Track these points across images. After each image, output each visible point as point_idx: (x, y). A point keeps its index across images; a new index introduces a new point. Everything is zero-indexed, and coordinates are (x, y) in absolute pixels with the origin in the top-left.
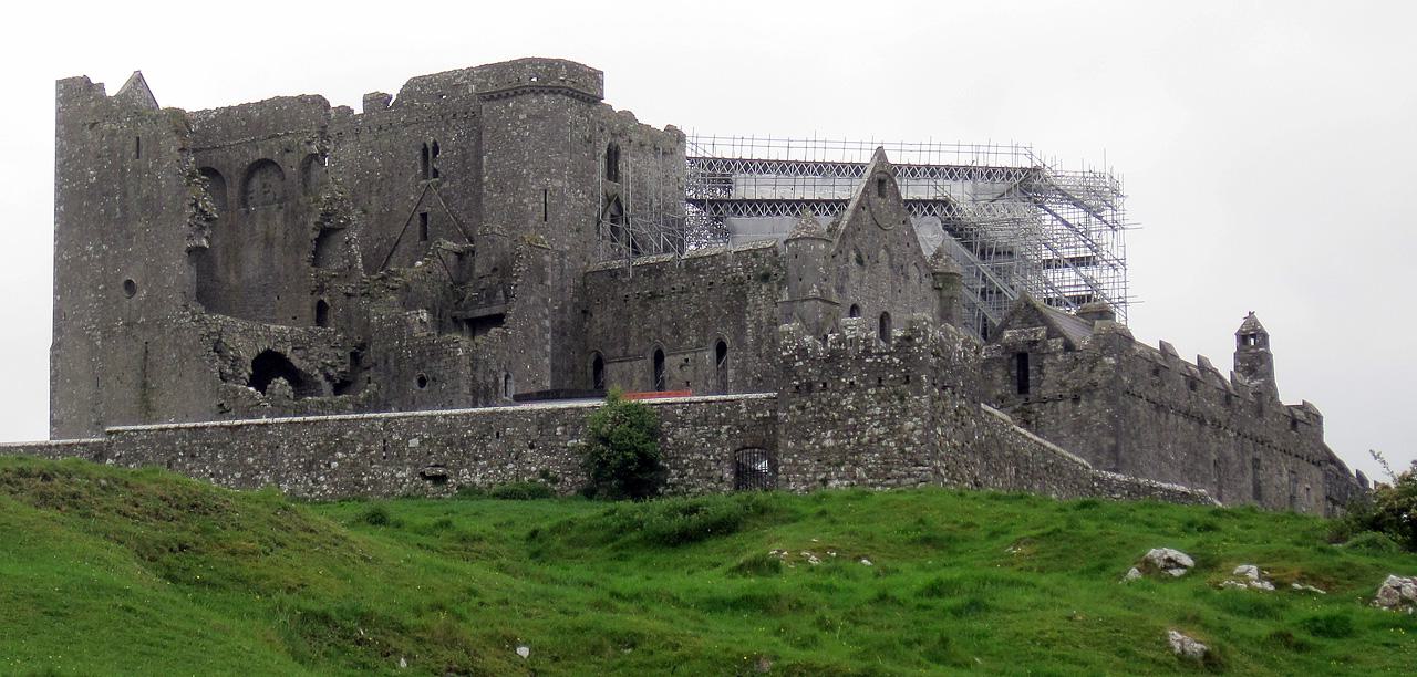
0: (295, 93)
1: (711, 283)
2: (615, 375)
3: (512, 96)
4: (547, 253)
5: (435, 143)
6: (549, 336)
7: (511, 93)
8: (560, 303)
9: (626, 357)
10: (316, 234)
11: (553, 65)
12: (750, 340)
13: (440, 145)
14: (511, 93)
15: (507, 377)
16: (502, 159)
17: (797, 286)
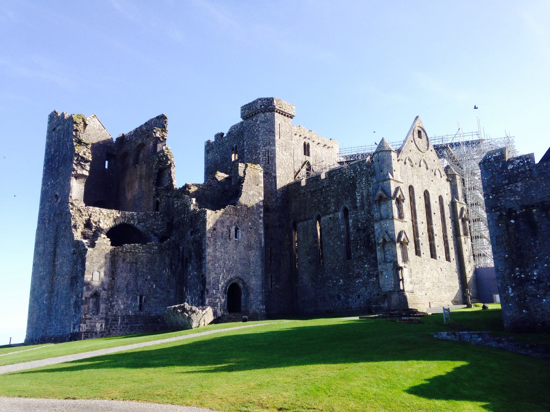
1: (339, 181)
5: (236, 146)
6: (262, 210)
8: (275, 198)
10: (157, 171)
12: (358, 205)
13: (237, 146)
15: (236, 230)
16: (251, 142)
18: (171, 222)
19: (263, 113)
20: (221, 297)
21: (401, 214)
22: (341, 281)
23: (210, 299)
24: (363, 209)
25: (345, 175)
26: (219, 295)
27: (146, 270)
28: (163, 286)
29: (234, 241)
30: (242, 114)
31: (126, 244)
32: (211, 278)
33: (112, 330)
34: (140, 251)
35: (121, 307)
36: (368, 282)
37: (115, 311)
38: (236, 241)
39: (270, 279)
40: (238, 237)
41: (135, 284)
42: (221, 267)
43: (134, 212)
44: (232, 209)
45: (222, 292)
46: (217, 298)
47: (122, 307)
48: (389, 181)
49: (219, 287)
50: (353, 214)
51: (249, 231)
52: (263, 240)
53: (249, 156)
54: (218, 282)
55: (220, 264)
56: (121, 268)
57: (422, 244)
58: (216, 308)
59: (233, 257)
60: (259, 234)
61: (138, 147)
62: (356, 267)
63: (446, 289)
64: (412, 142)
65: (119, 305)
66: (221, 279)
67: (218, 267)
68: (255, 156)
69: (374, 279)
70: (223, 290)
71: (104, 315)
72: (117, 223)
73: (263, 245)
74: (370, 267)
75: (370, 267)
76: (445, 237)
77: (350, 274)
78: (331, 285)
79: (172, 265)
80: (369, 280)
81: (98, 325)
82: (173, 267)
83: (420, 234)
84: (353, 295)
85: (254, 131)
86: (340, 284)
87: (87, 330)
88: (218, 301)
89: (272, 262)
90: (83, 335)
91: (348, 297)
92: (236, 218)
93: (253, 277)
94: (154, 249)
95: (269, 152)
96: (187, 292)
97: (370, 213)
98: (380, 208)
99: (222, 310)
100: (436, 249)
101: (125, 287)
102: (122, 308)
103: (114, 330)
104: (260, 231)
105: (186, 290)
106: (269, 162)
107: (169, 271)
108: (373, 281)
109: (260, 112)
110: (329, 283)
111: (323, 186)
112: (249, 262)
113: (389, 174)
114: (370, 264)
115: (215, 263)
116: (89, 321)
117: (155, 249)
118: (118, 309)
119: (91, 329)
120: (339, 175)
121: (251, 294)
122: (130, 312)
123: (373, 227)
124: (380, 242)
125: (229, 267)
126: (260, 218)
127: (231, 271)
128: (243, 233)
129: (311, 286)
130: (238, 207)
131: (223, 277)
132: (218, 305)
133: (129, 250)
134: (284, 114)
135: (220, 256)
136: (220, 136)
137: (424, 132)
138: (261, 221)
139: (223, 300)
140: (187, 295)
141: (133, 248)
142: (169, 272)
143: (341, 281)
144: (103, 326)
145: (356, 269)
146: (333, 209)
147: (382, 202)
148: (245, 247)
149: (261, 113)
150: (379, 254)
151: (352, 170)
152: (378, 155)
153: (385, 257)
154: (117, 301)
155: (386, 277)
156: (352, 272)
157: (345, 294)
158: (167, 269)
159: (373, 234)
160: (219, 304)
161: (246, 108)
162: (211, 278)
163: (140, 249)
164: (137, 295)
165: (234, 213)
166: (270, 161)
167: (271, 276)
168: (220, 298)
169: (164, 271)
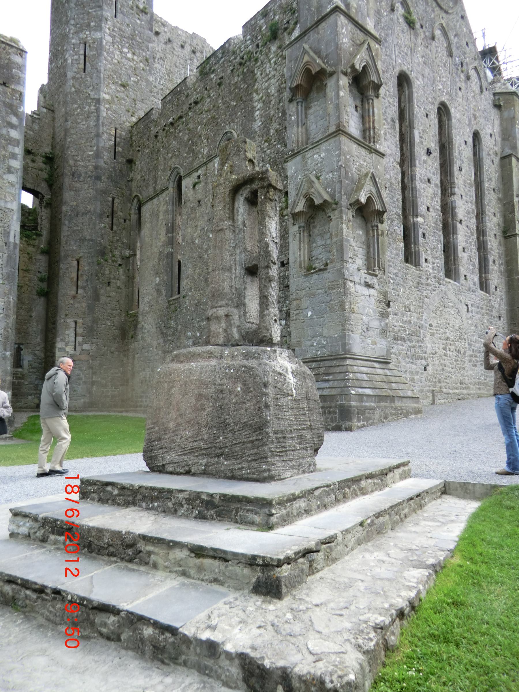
1: (221, 78)
57: (424, 235)
63: (476, 356)
76: (481, 232)
83: (422, 209)
100: (460, 256)
124: (297, 210)
146: (205, 152)
147: (314, 95)
151: (248, 37)
155: (310, 314)
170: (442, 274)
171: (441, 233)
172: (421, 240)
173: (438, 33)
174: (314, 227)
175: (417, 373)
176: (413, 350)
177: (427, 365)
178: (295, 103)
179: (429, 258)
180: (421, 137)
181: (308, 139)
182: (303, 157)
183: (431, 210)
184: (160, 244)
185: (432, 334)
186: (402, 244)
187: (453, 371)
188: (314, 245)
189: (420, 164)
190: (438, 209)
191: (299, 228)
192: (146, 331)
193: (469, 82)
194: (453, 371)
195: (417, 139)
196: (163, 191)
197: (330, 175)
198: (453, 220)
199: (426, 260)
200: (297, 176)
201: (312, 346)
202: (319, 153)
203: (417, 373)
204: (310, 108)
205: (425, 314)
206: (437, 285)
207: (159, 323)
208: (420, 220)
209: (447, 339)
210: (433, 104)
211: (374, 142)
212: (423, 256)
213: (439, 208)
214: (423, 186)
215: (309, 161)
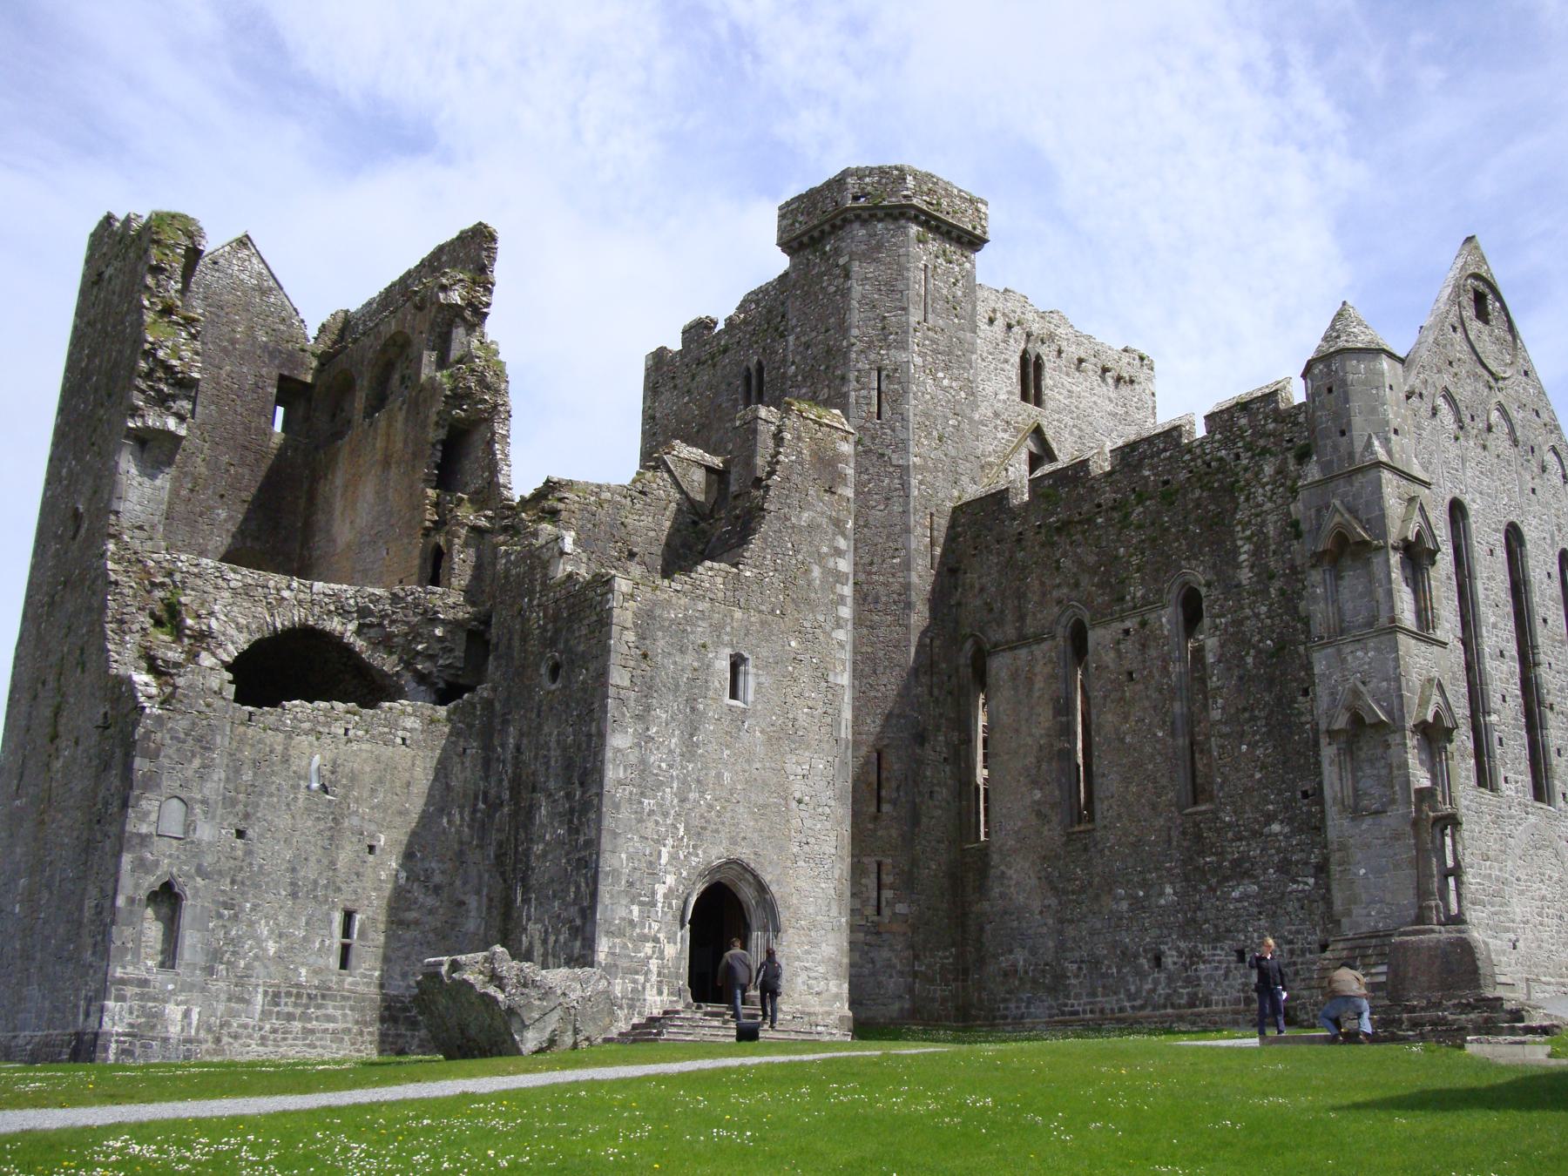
0: (453, 234)
1: (1166, 483)
2: (1004, 674)
3: (830, 233)
4: (846, 439)
5: (759, 363)
6: (847, 590)
7: (827, 227)
9: (1023, 640)
10: (442, 434)
11: (893, 176)
13: (764, 363)
14: (827, 227)
15: (737, 663)
16: (814, 334)
17: (1335, 448)
18: (482, 627)
19: (864, 222)
20: (661, 936)
21: (1426, 609)
22: (1169, 890)
23: (617, 940)
24: (1266, 591)
25: (1187, 457)
26: (655, 926)
27: (372, 808)
28: (437, 878)
29: (726, 709)
30: (782, 230)
31: (297, 702)
32: (624, 856)
33: (229, 1035)
34: (351, 733)
35: (265, 950)
36: (1283, 894)
37: (242, 964)
38: (731, 708)
39: (873, 877)
40: (741, 693)
41: (325, 862)
42: (665, 815)
43: (345, 587)
44: (719, 580)
45: (669, 917)
46: (644, 938)
47: (272, 947)
48: (1372, 474)
49: (653, 893)
50: (1224, 616)
51: (791, 674)
52: (847, 714)
53: (804, 391)
54: (654, 875)
55: (663, 799)
56: (271, 795)
57: (1500, 739)
58: (641, 978)
59: (719, 776)
60: (833, 689)
61: (384, 349)
62: (1230, 835)
64: (1454, 329)
65: (259, 941)
66: (664, 861)
67: (651, 812)
68: (826, 390)
69: (1306, 884)
70: (670, 906)
71: (198, 972)
72: (279, 625)
73: (846, 733)
74: (1293, 833)
75: (1293, 833)
77: (1206, 863)
78: (1124, 906)
79: (476, 798)
80: (1286, 886)
81: (174, 1011)
82: (481, 806)
83: (1495, 701)
84: (1215, 948)
85: (826, 294)
86: (1162, 902)
87: (131, 1025)
88: (650, 952)
89: (886, 808)
90: (113, 1045)
91: (1194, 956)
92: (738, 614)
93: (801, 863)
94: (405, 729)
95: (884, 373)
96: (529, 909)
97: (1296, 608)
98: (1337, 586)
99: (666, 991)
100: (1554, 763)
101: (287, 870)
102: (271, 952)
103: (236, 1037)
104: (836, 674)
105: (526, 901)
106: (883, 409)
107: (462, 818)
108: (1303, 891)
109: (851, 222)
110: (1118, 900)
111: (1099, 506)
112: (785, 799)
113: (1376, 443)
114: (1290, 821)
115: (643, 794)
116: (137, 990)
117: (411, 730)
118: (256, 957)
119: (147, 1023)
120: (1165, 459)
121: (791, 931)
122: (303, 971)
123: (1308, 667)
125: (702, 816)
126: (839, 626)
127: (708, 833)
128: (762, 679)
129: (1041, 912)
130: (748, 574)
131: (673, 857)
132: (649, 970)
133: (307, 725)
134: (944, 228)
135: (664, 765)
136: (698, 331)
137: (1499, 298)
138: (841, 635)
139: (670, 951)
140: (529, 919)
141: (321, 719)
142: (461, 826)
143: (1169, 890)
144: (195, 1017)
145: (1233, 840)
148: (770, 739)
149: (856, 225)
150: (1330, 773)
152: (1328, 367)
153: (1356, 790)
154: (251, 924)
155: (1362, 871)
156: (1213, 854)
157: (1182, 945)
158: (455, 811)
159: (1306, 693)
160: (654, 965)
161: (797, 209)
162: (624, 856)
163: (348, 723)
164: (334, 906)
165: (728, 593)
166: (885, 407)
167: (879, 865)
168: (656, 940)
169: (445, 820)
170: (1530, 797)
171: (1524, 733)
172: (1498, 751)
173: (1495, 416)
174: (1360, 749)
175: (1504, 952)
176: (1496, 917)
177: (1517, 940)
178: (1321, 570)
179: (1510, 775)
180: (1486, 589)
181: (1342, 621)
182: (1339, 651)
183: (1507, 699)
184: (1037, 731)
185: (1522, 893)
186: (1473, 761)
187: (1553, 948)
188: (1360, 774)
189: (1488, 631)
190: (1517, 696)
191: (1339, 749)
192: (1013, 882)
193: (1545, 475)
194: (1553, 948)
195: (1481, 594)
196: (1039, 639)
197: (1385, 684)
198: (1539, 706)
199: (1506, 779)
200: (1331, 675)
201: (1369, 915)
202: (1365, 650)
203: (1504, 952)
204: (1342, 578)
205: (1509, 863)
206: (1524, 815)
207: (1045, 869)
208: (1494, 718)
209: (1543, 898)
210: (1497, 530)
211: (1434, 628)
212: (1502, 772)
213: (1519, 693)
214: (1496, 663)
215: (1349, 658)
